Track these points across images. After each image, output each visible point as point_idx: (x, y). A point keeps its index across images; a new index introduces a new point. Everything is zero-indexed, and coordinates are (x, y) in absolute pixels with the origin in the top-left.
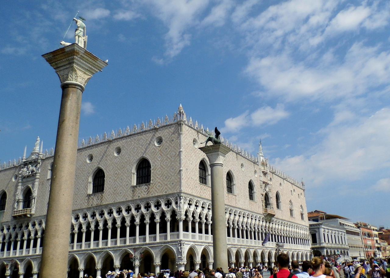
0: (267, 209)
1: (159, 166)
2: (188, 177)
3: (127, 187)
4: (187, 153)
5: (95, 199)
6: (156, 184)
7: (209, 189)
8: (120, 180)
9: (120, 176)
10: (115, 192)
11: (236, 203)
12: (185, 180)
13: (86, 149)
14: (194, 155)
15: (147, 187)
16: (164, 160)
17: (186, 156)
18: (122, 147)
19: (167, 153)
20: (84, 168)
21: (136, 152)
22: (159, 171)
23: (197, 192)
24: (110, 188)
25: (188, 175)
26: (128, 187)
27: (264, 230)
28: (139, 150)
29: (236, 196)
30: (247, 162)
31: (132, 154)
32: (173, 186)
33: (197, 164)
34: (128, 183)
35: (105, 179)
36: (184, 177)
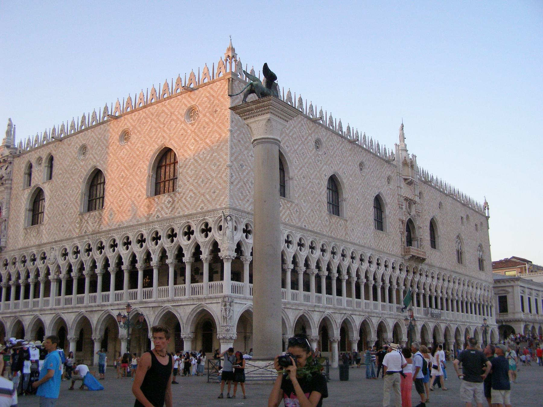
0: (409, 248)
1: (192, 160)
2: (245, 181)
4: (242, 135)
5: (90, 223)
6: (187, 193)
8: (129, 188)
9: (128, 181)
10: (120, 210)
11: (346, 234)
12: (238, 187)
15: (171, 200)
16: (200, 149)
17: (239, 141)
18: (132, 129)
21: (155, 137)
22: (192, 170)
24: (112, 203)
25: (245, 177)
26: (140, 201)
27: (402, 284)
28: (159, 133)
29: (346, 221)
31: (147, 140)
32: (214, 196)
34: (140, 193)
35: (106, 187)
36: (235, 180)
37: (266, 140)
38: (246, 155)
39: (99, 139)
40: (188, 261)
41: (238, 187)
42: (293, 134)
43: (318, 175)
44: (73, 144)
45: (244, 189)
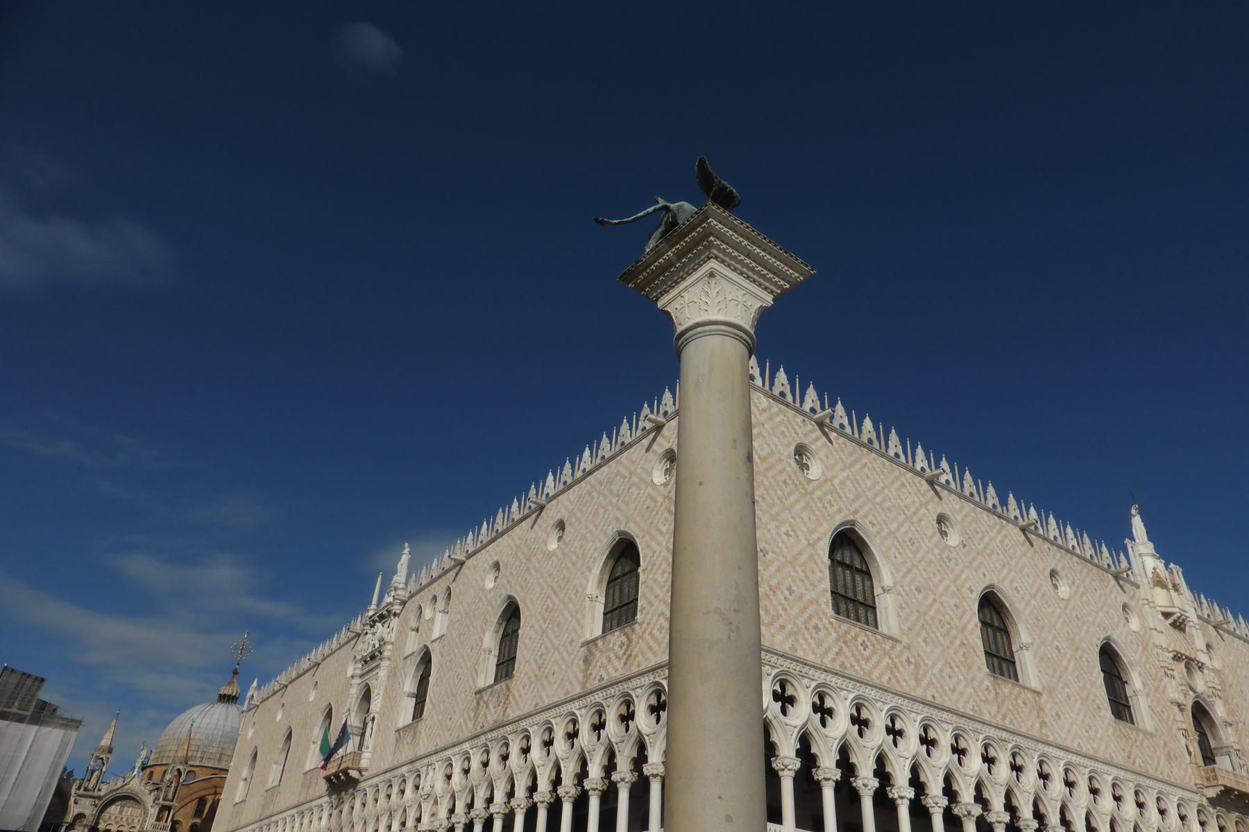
0: (1214, 770)
3: (570, 649)
5: (491, 707)
7: (887, 647)
11: (1043, 724)
14: (802, 504)
15: (624, 639)
22: (664, 572)
23: (822, 649)
24: (528, 662)
29: (1038, 693)
30: (1078, 568)
31: (591, 532)
33: (819, 539)
35: (520, 631)
37: (706, 328)
38: (774, 532)
39: (518, 547)
40: (655, 772)
42: (884, 500)
43: (953, 588)
45: (771, 601)
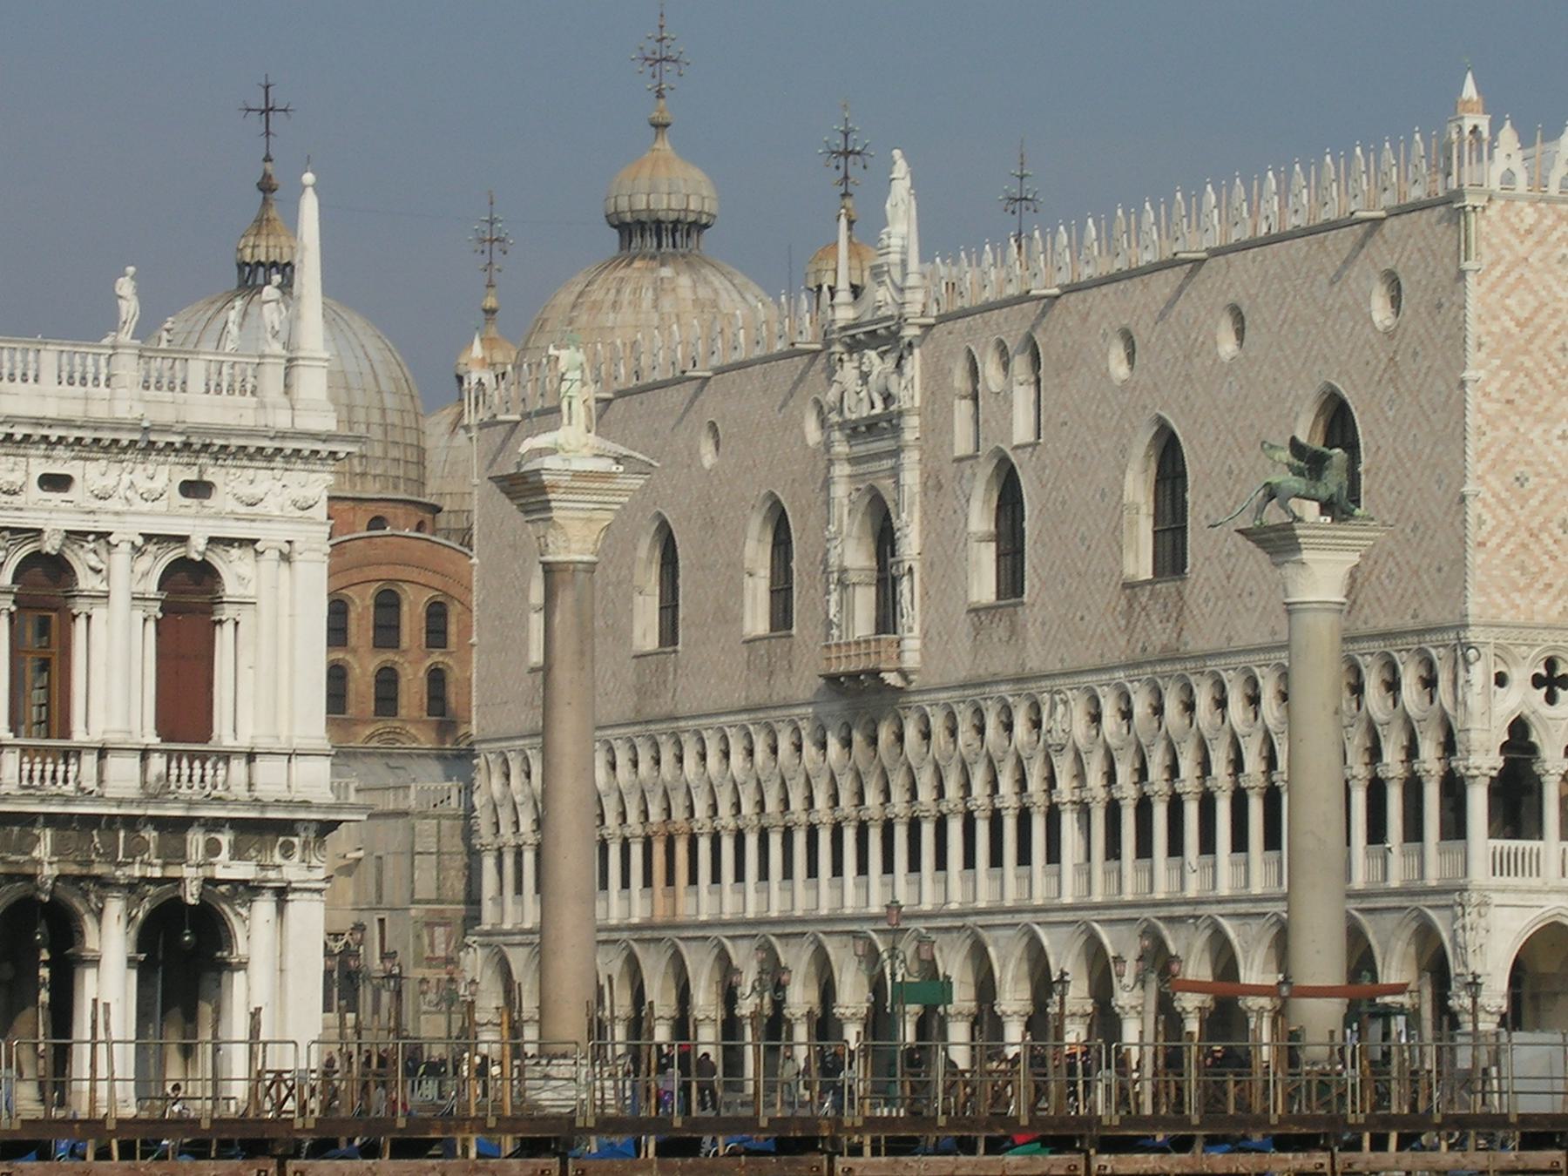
1: (1391, 456)
2: (1535, 524)
4: (1521, 379)
5: (1154, 617)
12: (1505, 551)
13: (1104, 289)
17: (1508, 402)
19: (1419, 381)
20: (1103, 415)
22: (1391, 489)
24: (1207, 559)
25: (1534, 514)
31: (1286, 358)
36: (1491, 534)
38: (1539, 442)
41: (1505, 551)
44: (1093, 318)
